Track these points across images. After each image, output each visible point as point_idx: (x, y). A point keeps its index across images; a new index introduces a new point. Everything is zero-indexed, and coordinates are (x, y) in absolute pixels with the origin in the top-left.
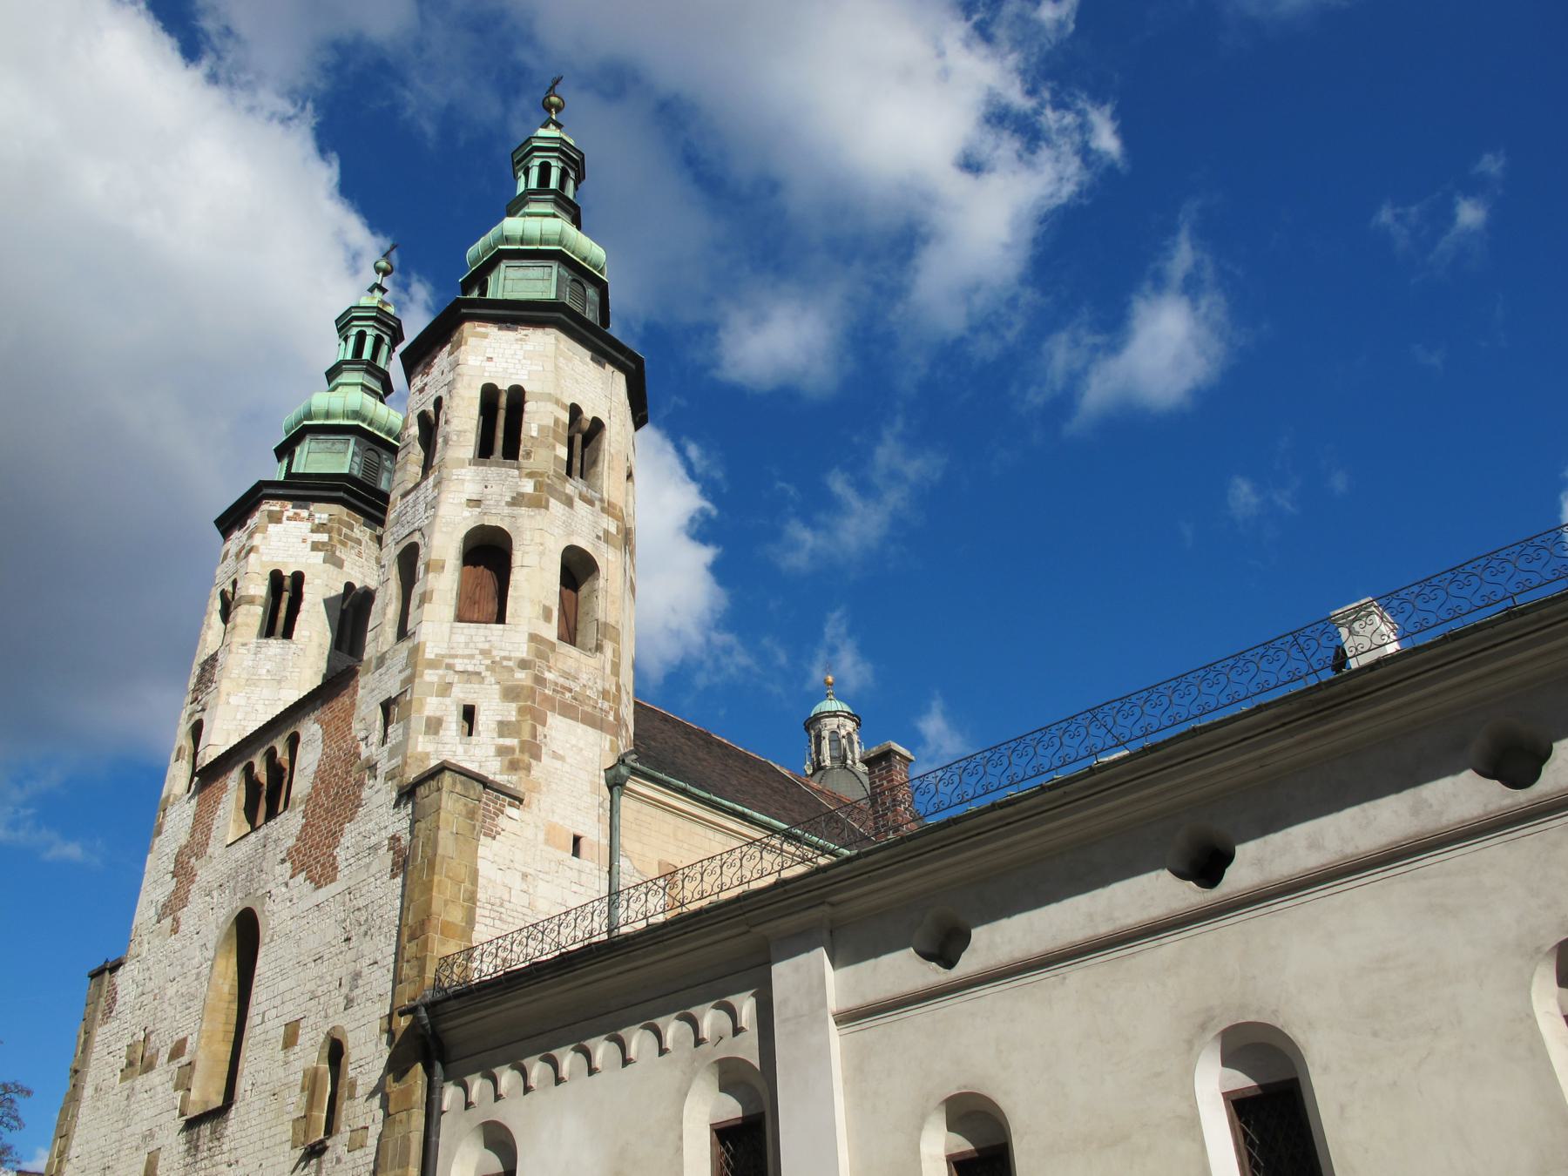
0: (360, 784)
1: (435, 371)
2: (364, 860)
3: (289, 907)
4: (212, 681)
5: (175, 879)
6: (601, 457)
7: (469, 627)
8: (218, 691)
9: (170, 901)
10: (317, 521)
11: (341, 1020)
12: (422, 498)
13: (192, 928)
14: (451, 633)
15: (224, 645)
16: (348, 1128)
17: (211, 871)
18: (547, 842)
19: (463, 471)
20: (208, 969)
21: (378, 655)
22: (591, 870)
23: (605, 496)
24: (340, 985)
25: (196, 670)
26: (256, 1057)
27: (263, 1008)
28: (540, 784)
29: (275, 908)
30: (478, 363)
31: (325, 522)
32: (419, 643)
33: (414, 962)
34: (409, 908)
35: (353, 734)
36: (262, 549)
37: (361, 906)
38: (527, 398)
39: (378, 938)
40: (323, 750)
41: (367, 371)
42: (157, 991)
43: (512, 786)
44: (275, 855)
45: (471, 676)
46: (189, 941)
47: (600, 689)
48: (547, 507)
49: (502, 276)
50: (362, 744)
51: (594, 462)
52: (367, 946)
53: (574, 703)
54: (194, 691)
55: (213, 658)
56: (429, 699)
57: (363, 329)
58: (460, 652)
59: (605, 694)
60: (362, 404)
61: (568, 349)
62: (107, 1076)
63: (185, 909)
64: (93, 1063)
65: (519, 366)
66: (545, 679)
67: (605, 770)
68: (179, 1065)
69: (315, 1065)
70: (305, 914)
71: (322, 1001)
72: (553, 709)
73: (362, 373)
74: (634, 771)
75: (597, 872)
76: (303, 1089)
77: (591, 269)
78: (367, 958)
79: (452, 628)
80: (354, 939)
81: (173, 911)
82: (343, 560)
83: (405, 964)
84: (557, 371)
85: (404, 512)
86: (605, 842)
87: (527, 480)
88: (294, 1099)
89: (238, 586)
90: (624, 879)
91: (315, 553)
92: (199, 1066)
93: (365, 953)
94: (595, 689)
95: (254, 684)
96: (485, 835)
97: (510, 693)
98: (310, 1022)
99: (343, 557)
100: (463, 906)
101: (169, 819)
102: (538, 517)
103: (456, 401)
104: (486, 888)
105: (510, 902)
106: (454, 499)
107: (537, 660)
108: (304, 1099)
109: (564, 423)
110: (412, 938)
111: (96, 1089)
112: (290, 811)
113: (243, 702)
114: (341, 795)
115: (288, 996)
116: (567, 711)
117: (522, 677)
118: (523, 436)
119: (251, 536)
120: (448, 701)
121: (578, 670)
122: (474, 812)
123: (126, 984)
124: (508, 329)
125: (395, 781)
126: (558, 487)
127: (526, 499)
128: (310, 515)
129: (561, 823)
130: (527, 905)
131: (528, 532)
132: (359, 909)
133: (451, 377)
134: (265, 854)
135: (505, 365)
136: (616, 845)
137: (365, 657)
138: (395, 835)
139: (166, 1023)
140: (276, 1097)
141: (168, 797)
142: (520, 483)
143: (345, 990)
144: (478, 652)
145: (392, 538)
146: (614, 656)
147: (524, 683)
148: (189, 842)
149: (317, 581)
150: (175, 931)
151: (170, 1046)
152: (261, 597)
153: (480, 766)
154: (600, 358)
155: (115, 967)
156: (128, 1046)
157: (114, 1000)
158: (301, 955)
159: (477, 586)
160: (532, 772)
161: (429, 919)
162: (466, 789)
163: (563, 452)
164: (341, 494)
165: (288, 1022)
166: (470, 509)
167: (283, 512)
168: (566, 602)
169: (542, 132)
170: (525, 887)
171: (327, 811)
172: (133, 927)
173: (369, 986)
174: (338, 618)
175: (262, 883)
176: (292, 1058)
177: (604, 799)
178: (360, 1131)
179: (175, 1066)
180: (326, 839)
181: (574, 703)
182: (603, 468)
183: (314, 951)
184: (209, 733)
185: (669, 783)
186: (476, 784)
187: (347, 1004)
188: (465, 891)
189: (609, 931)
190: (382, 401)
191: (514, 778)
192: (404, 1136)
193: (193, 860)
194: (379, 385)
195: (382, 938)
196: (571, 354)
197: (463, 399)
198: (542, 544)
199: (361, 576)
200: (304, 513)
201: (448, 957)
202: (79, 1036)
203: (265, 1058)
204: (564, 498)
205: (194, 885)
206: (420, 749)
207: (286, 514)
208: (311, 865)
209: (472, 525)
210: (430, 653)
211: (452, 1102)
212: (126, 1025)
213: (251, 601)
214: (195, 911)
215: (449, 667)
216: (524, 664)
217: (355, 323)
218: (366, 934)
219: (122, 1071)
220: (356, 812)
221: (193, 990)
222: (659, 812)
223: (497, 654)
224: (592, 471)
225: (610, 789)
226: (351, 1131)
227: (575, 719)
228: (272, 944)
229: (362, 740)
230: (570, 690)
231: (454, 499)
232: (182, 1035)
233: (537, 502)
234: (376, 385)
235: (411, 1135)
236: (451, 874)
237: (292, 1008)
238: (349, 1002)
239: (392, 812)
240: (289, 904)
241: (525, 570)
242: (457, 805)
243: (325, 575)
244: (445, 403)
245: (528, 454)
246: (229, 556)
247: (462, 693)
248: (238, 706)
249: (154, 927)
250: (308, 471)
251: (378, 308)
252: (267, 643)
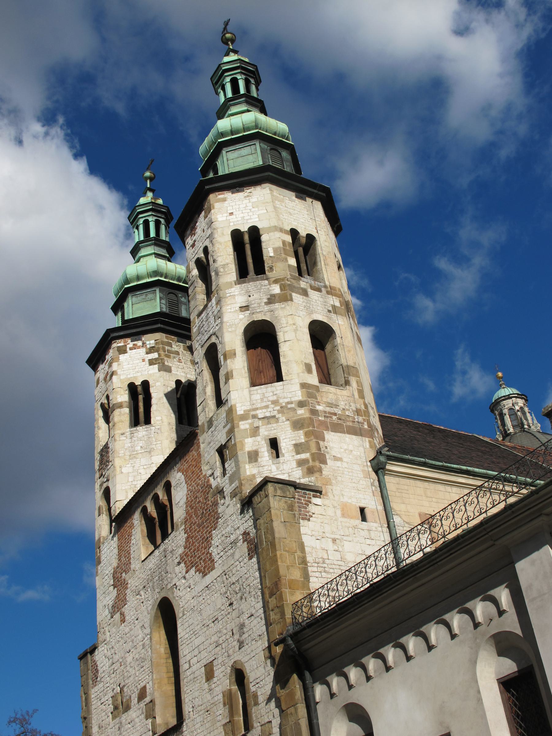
0: (216, 504)
1: (199, 231)
2: (229, 551)
3: (189, 592)
4: (108, 462)
5: (116, 589)
6: (318, 259)
7: (261, 389)
8: (114, 467)
9: (116, 603)
10: (148, 346)
11: (238, 656)
12: (210, 313)
13: (133, 617)
14: (250, 395)
15: (111, 437)
16: (259, 724)
17: (136, 579)
18: (343, 515)
19: (233, 289)
20: (149, 640)
21: (208, 419)
22: (376, 528)
23: (327, 283)
24: (233, 634)
25: (97, 457)
26: (191, 689)
27: (188, 658)
28: (330, 479)
29: (181, 593)
30: (224, 219)
31: (153, 345)
32: (231, 406)
33: (277, 610)
34: (265, 576)
35: (204, 474)
36: (119, 372)
37: (234, 581)
38: (261, 232)
39: (250, 599)
40: (187, 488)
41: (155, 244)
42: (121, 660)
43: (313, 484)
44: (173, 560)
45: (268, 419)
46: (133, 625)
47: (354, 409)
48: (291, 300)
49: (225, 159)
50: (211, 479)
51: (315, 263)
52: (244, 606)
53: (340, 422)
54: (99, 470)
55: (106, 447)
56: (246, 440)
57: (146, 218)
58: (259, 406)
59: (358, 412)
60: (158, 266)
61: (279, 194)
62: (104, 718)
63: (126, 606)
64: (93, 711)
65: (251, 214)
66: (317, 410)
67: (370, 461)
68: (145, 703)
69: (228, 688)
70: (201, 594)
71: (224, 647)
72: (327, 429)
73: (153, 247)
74: (389, 458)
75: (380, 529)
76: (225, 705)
77: (281, 139)
78: (246, 613)
79: (250, 391)
80: (235, 603)
81: (119, 609)
82: (171, 367)
83: (271, 613)
84: (276, 210)
85: (201, 325)
86: (381, 508)
87: (274, 285)
88: (221, 712)
89: (110, 398)
90: (399, 529)
91: (152, 367)
92: (157, 702)
93: (244, 610)
94: (351, 410)
95: (135, 457)
96: (303, 519)
97: (297, 425)
98: (220, 662)
99: (170, 365)
100: (299, 568)
101: (103, 552)
102: (288, 307)
103: (217, 246)
104: (311, 553)
105: (328, 559)
106: (231, 309)
107: (309, 399)
108: (227, 711)
109: (289, 243)
110: (271, 595)
111: (99, 727)
112: (176, 531)
113: (131, 470)
114: (206, 514)
115: (202, 647)
116: (337, 428)
117: (302, 412)
118: (265, 258)
119: (110, 366)
120: (259, 438)
121: (337, 400)
122: (292, 505)
123: (101, 659)
124: (238, 191)
125: (238, 497)
126: (296, 285)
127: (277, 298)
128: (143, 343)
129: (350, 501)
130: (340, 559)
131: (283, 319)
132: (233, 584)
133: (209, 232)
134: (167, 561)
135: (242, 215)
136: (388, 508)
137: (200, 423)
138: (245, 532)
139: (131, 679)
140: (209, 712)
141: (99, 539)
142: (270, 288)
143: (237, 637)
144: (270, 403)
145: (198, 344)
146: (358, 386)
147: (305, 416)
148: (118, 564)
149: (158, 384)
150: (123, 621)
151: (137, 692)
152: (126, 402)
153: (289, 476)
154: (302, 195)
155: (93, 650)
156: (111, 697)
157: (97, 671)
158: (204, 620)
159: (259, 362)
160: (324, 473)
161: (279, 580)
162: (284, 492)
163: (293, 261)
164: (159, 325)
165: (205, 664)
166: (243, 313)
167: (126, 345)
168: (318, 358)
169: (226, 59)
170: (336, 548)
171: (199, 526)
172: (98, 623)
173: (250, 632)
174: (176, 403)
175: (169, 580)
176: (213, 686)
177: (374, 480)
178: (267, 725)
179: (142, 704)
180: (203, 543)
181: (340, 422)
182: (321, 266)
183: (211, 617)
184: (115, 493)
185: (413, 460)
186: (289, 487)
187: (240, 645)
188: (298, 558)
189: (398, 564)
190: (169, 261)
191: (313, 479)
192: (295, 723)
193: (124, 575)
194: (165, 251)
195: (252, 598)
196: (282, 197)
197: (221, 244)
198: (294, 324)
199: (183, 374)
200: (139, 343)
201: (297, 602)
202: (81, 697)
203: (196, 689)
204: (301, 291)
205: (128, 590)
207: (128, 346)
208: (197, 562)
209: (246, 322)
210: (240, 411)
211: (321, 696)
212: (108, 685)
213: (120, 406)
214: (132, 606)
215: (254, 417)
216: (301, 404)
217: (140, 216)
218: (241, 598)
219: (112, 713)
220: (217, 523)
221: (142, 656)
222: (412, 481)
223: (283, 401)
224: (314, 269)
225: (376, 472)
226: (261, 726)
227: (343, 432)
228: (185, 617)
229: (210, 476)
230: (335, 414)
231: (231, 309)
232: (142, 685)
233: (285, 298)
234: (163, 252)
235: (300, 721)
236: (287, 549)
237: (206, 655)
238: (241, 645)
239: (240, 517)
240: (189, 590)
241: (288, 343)
242: (280, 503)
243: (162, 378)
244: (210, 249)
245: (271, 269)
246: (100, 381)
247: (266, 432)
248: (128, 473)
249: (110, 622)
250: (135, 316)
251: (152, 202)
252: (136, 430)
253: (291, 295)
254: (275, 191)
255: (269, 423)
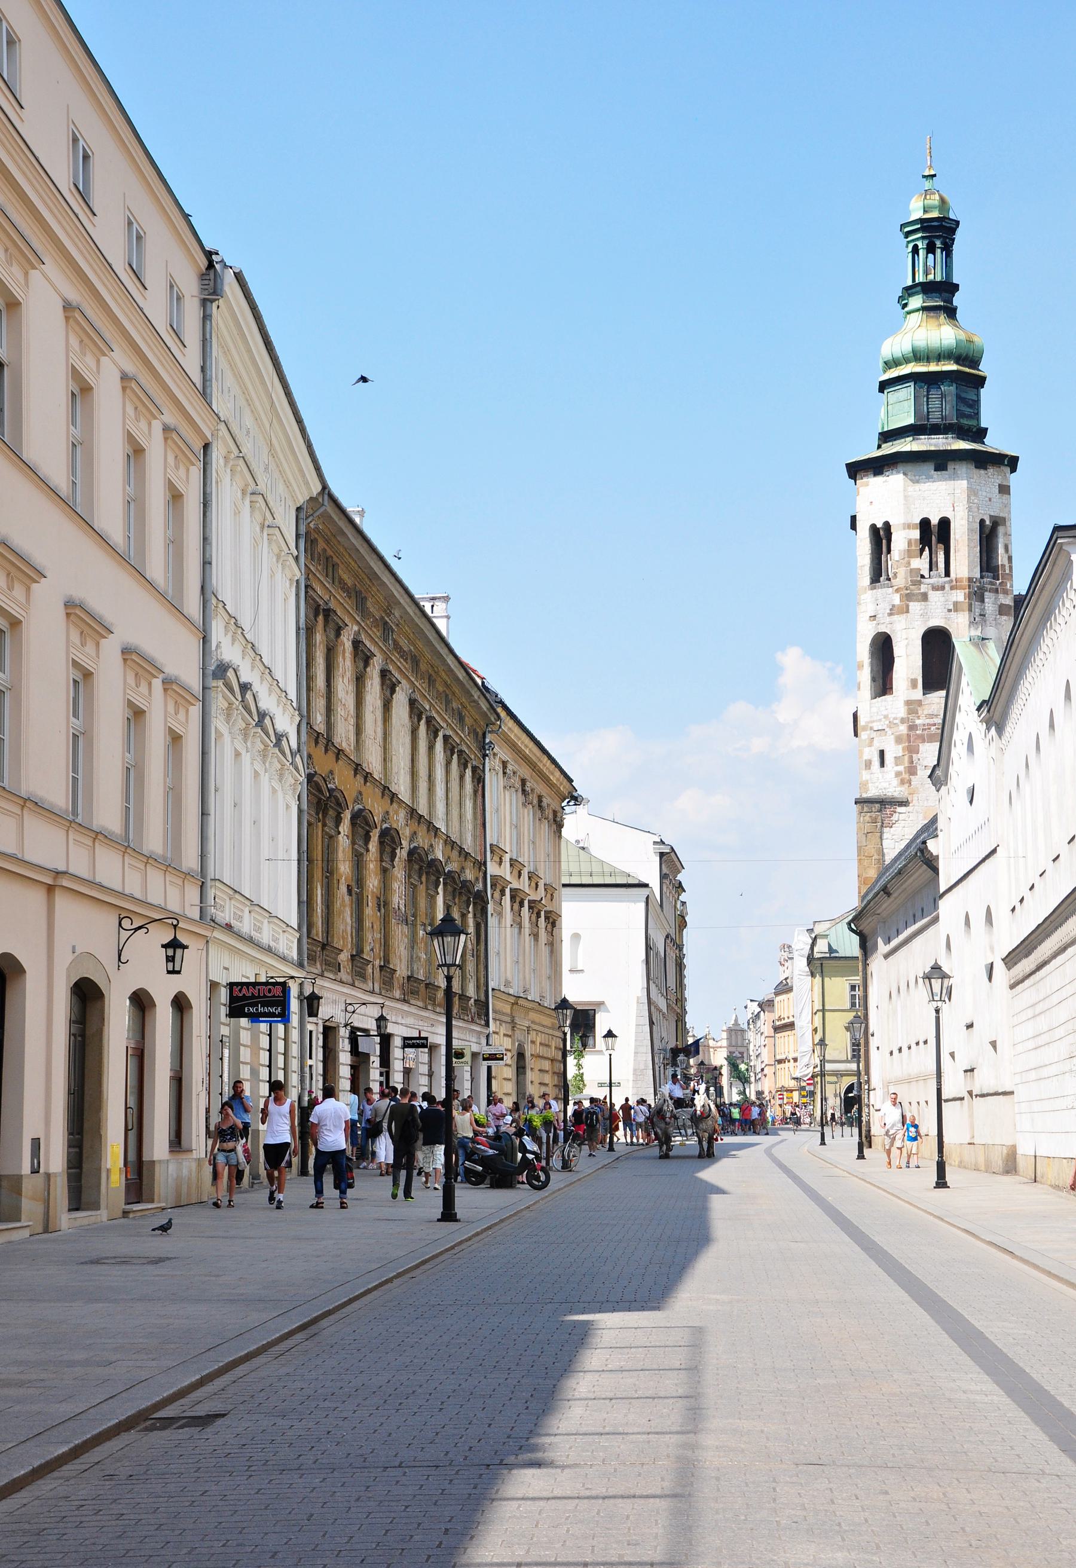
14: (871, 707)
48: (907, 612)
79: (870, 704)
96: (886, 827)
97: (898, 740)
142: (893, 598)
144: (882, 717)
166: (871, 623)
191: (902, 789)
198: (907, 639)
206: (864, 779)
216: (903, 721)
230: (935, 725)
247: (878, 745)
253: (908, 606)
254: (909, 474)
255: (880, 735)
